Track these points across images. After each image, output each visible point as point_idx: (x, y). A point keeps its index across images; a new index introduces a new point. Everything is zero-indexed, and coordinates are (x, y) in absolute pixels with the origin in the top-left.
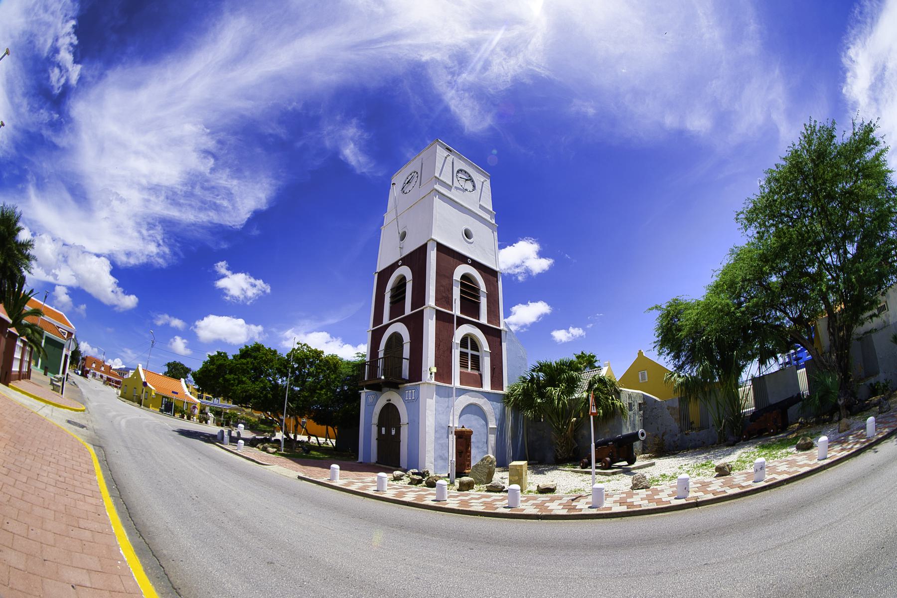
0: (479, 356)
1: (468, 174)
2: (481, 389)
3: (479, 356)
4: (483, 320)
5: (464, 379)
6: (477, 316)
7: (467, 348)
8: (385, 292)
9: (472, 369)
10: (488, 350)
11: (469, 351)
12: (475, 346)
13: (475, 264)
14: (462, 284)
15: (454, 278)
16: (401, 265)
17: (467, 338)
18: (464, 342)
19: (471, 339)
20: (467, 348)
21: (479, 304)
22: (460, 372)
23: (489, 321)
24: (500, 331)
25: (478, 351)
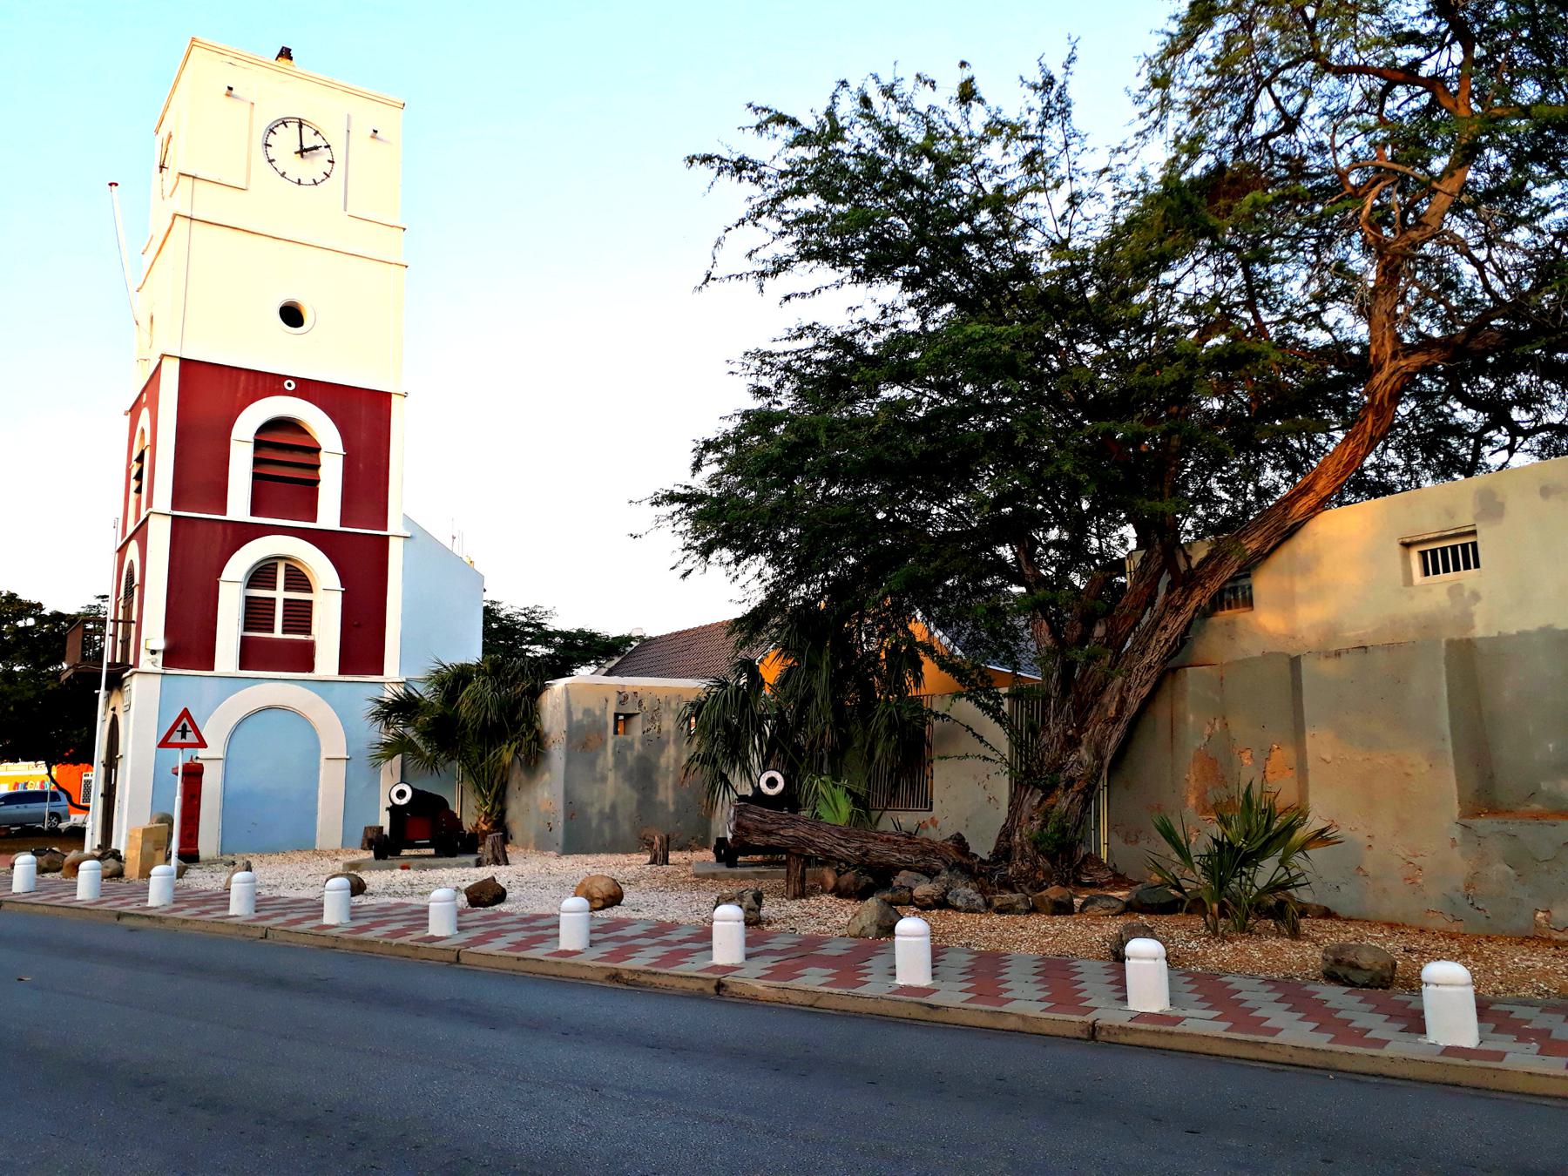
0: (311, 602)
2: (311, 674)
3: (311, 602)
4: (329, 515)
5: (253, 655)
6: (312, 515)
7: (274, 588)
9: (284, 632)
10: (339, 587)
11: (280, 594)
12: (298, 579)
13: (307, 389)
14: (258, 444)
17: (276, 564)
18: (262, 575)
19: (287, 565)
20: (274, 588)
21: (314, 483)
22: (245, 642)
24: (387, 537)
25: (310, 591)
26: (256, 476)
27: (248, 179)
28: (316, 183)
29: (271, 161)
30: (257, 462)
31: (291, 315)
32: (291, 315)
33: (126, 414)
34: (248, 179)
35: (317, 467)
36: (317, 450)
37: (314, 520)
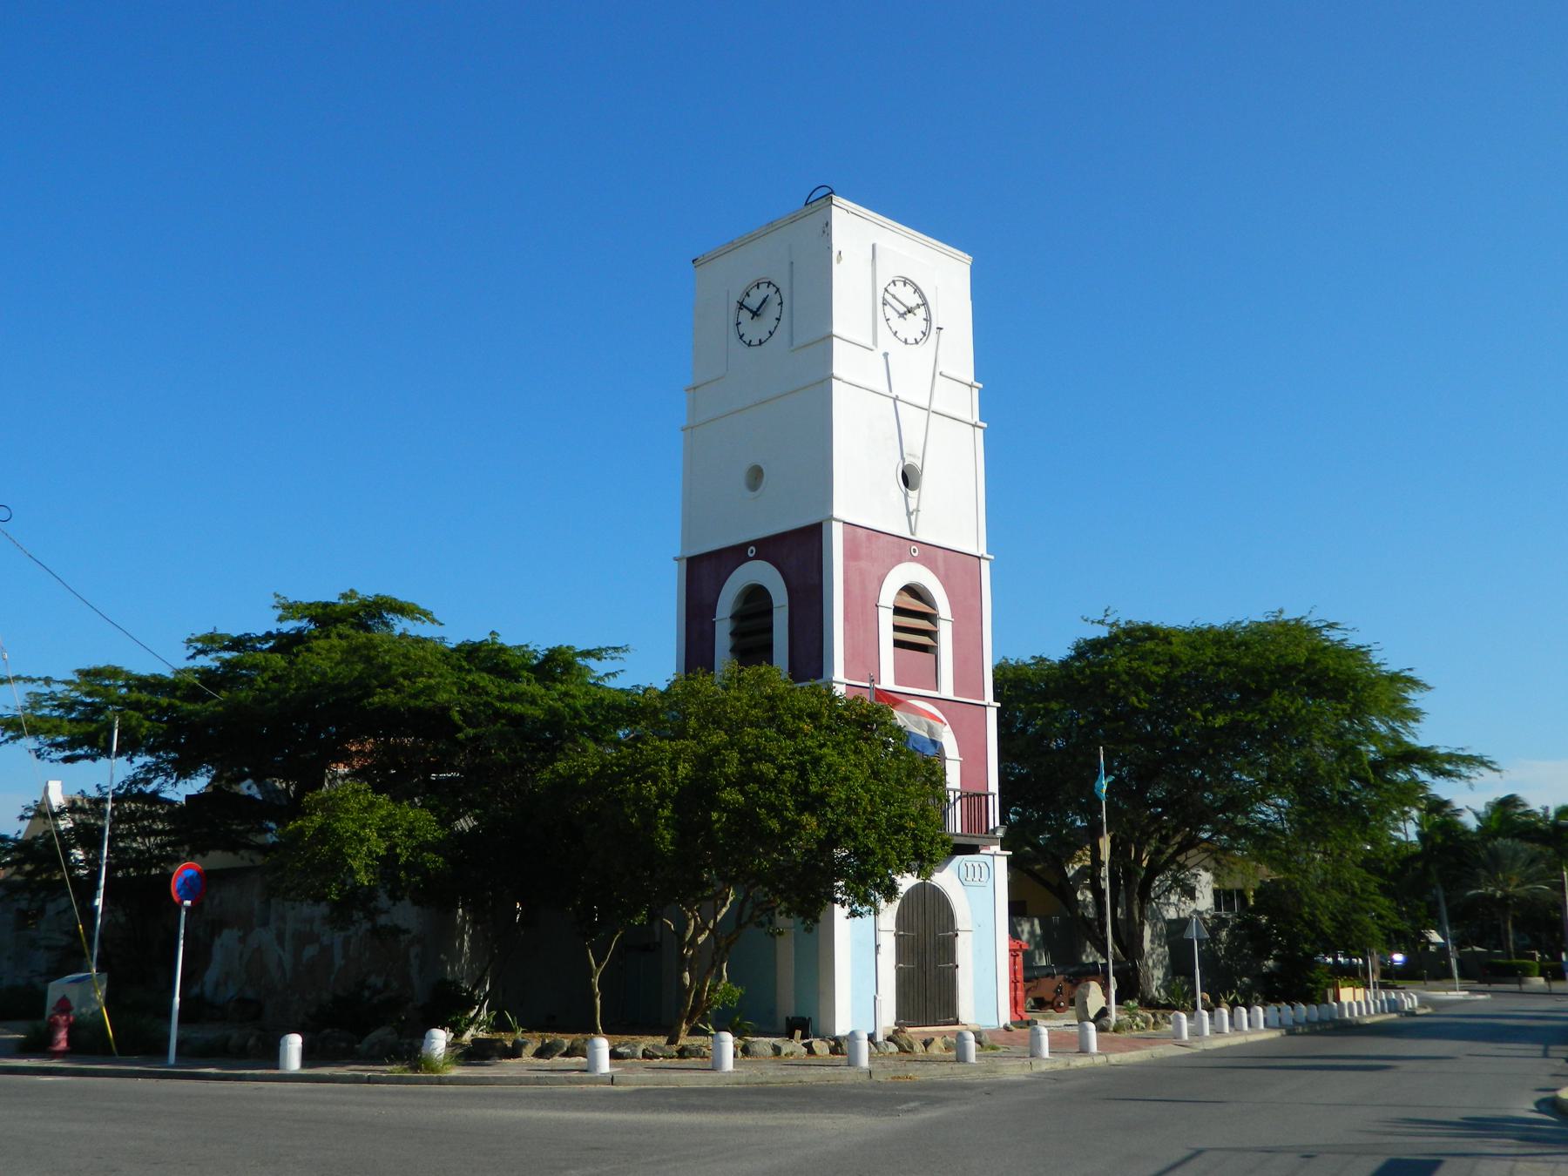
1: (913, 284)
8: (715, 617)
10: (957, 757)
13: (930, 554)
14: (898, 611)
15: (881, 603)
16: (755, 558)
23: (955, 695)
24: (985, 706)
26: (898, 644)
27: (875, 342)
28: (917, 342)
29: (888, 320)
30: (897, 628)
31: (909, 479)
32: (909, 479)
33: (675, 559)
34: (875, 342)
35: (932, 634)
36: (931, 618)
37: (937, 687)
